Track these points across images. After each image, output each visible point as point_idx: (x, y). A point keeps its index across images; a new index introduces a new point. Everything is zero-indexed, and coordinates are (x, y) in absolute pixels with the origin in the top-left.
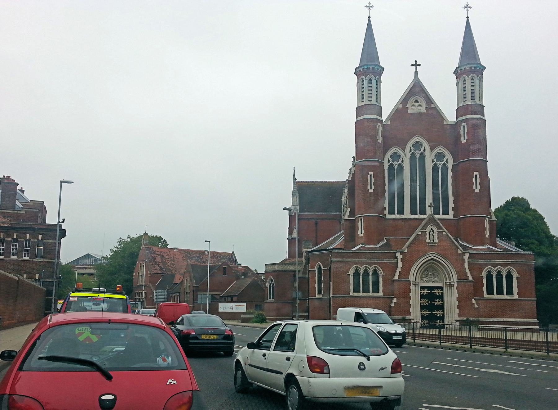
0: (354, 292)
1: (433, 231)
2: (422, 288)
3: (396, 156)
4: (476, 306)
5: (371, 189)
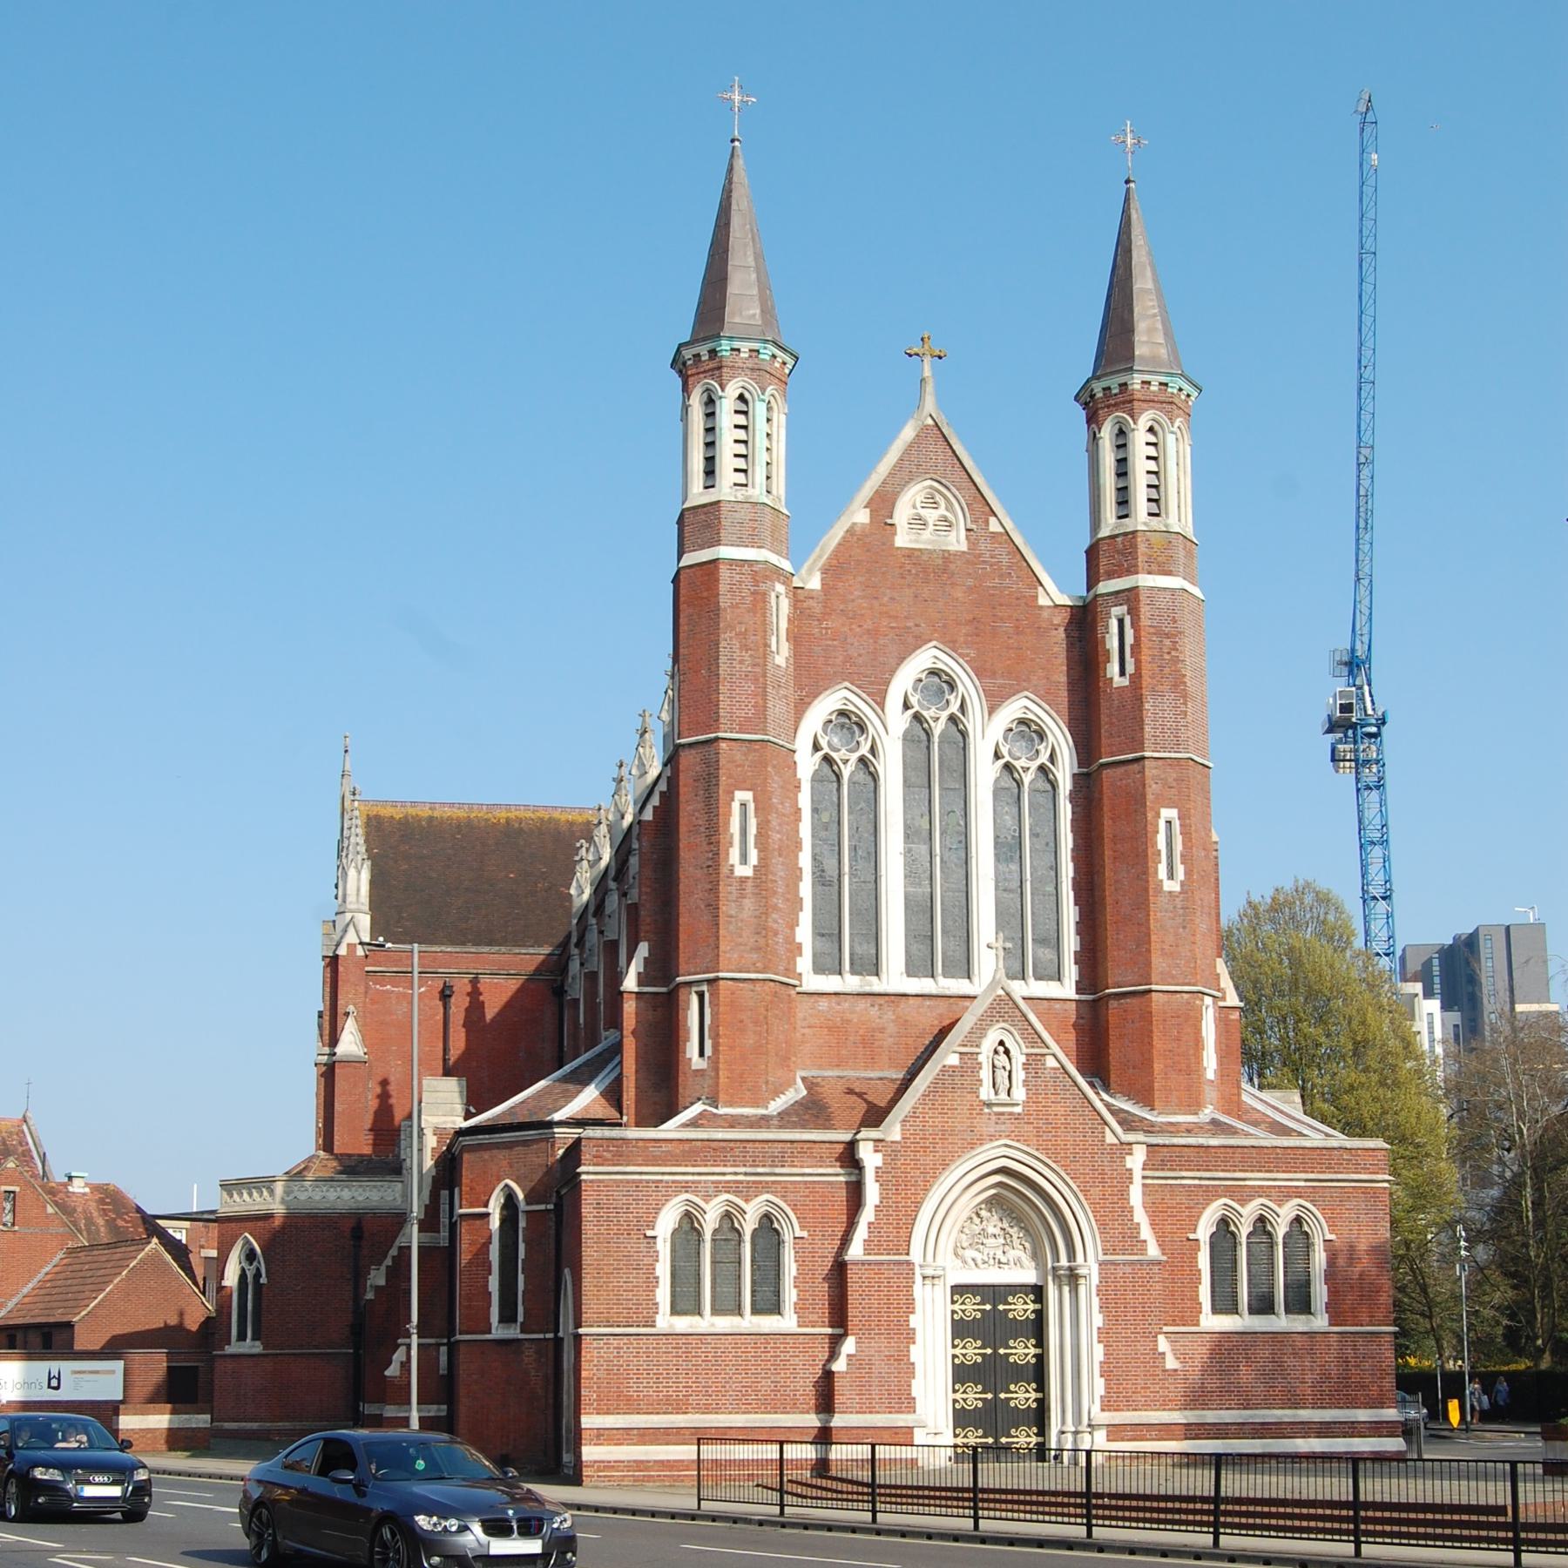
0: (675, 1311)
1: (1007, 1052)
2: (959, 1290)
5: (744, 859)
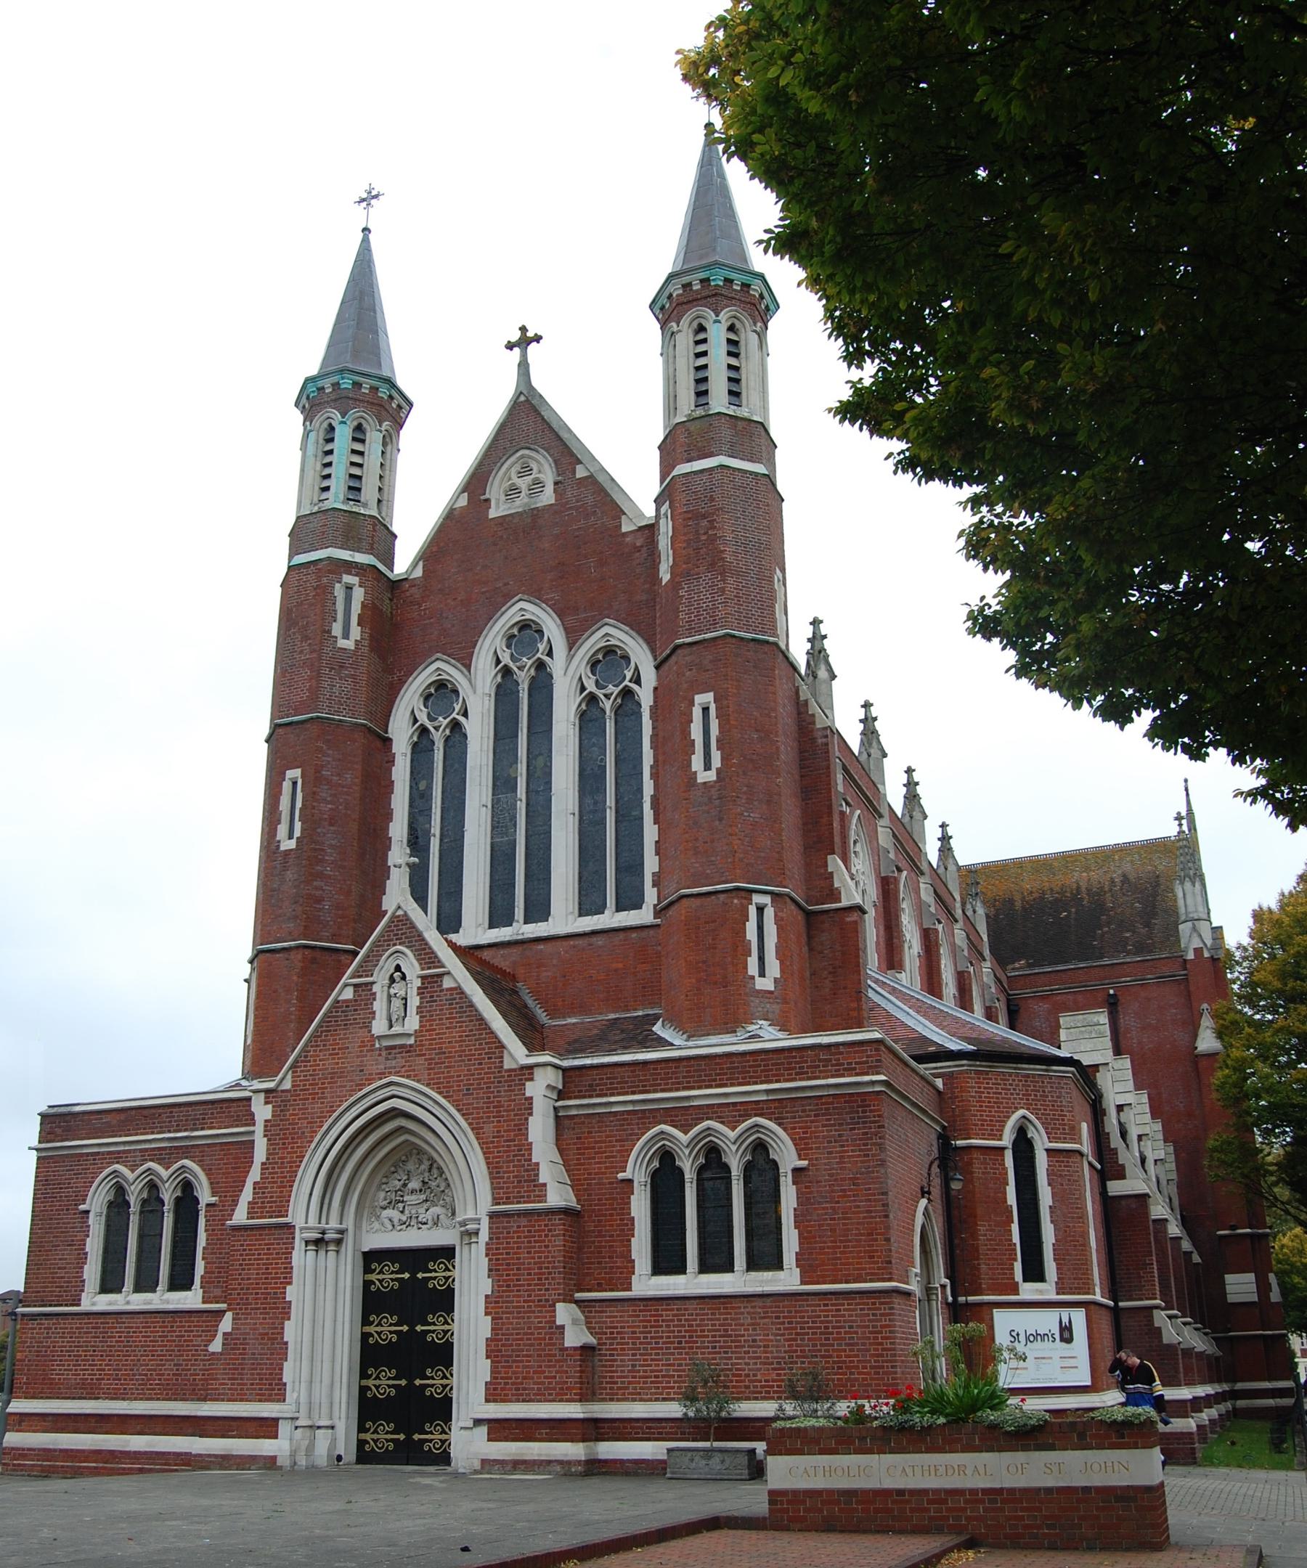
1: (404, 977)
3: (442, 692)
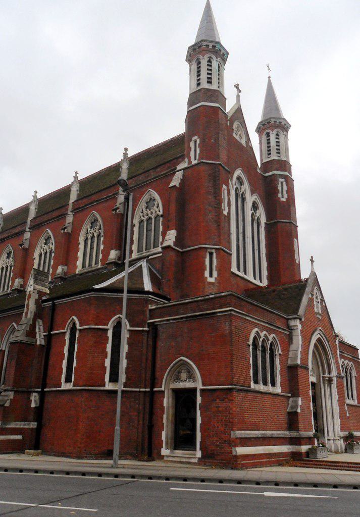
4: (348, 415)
